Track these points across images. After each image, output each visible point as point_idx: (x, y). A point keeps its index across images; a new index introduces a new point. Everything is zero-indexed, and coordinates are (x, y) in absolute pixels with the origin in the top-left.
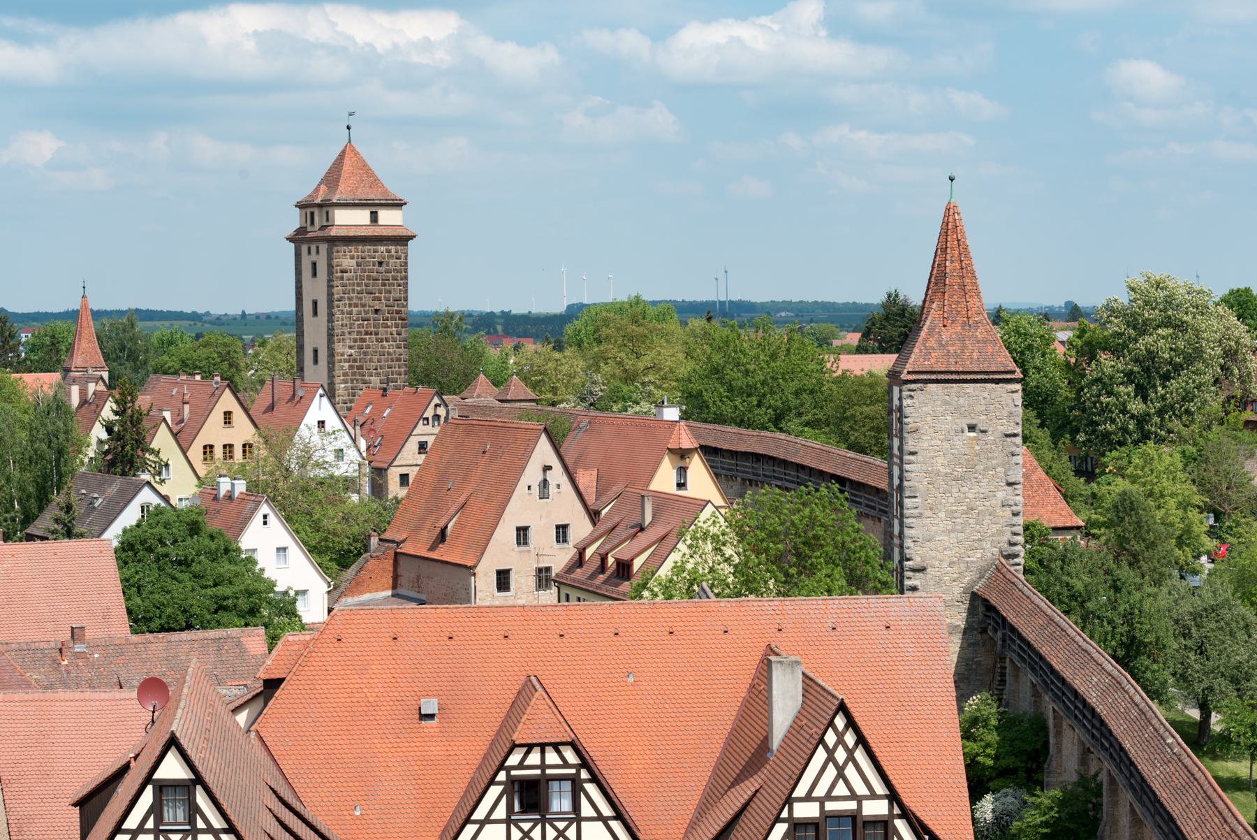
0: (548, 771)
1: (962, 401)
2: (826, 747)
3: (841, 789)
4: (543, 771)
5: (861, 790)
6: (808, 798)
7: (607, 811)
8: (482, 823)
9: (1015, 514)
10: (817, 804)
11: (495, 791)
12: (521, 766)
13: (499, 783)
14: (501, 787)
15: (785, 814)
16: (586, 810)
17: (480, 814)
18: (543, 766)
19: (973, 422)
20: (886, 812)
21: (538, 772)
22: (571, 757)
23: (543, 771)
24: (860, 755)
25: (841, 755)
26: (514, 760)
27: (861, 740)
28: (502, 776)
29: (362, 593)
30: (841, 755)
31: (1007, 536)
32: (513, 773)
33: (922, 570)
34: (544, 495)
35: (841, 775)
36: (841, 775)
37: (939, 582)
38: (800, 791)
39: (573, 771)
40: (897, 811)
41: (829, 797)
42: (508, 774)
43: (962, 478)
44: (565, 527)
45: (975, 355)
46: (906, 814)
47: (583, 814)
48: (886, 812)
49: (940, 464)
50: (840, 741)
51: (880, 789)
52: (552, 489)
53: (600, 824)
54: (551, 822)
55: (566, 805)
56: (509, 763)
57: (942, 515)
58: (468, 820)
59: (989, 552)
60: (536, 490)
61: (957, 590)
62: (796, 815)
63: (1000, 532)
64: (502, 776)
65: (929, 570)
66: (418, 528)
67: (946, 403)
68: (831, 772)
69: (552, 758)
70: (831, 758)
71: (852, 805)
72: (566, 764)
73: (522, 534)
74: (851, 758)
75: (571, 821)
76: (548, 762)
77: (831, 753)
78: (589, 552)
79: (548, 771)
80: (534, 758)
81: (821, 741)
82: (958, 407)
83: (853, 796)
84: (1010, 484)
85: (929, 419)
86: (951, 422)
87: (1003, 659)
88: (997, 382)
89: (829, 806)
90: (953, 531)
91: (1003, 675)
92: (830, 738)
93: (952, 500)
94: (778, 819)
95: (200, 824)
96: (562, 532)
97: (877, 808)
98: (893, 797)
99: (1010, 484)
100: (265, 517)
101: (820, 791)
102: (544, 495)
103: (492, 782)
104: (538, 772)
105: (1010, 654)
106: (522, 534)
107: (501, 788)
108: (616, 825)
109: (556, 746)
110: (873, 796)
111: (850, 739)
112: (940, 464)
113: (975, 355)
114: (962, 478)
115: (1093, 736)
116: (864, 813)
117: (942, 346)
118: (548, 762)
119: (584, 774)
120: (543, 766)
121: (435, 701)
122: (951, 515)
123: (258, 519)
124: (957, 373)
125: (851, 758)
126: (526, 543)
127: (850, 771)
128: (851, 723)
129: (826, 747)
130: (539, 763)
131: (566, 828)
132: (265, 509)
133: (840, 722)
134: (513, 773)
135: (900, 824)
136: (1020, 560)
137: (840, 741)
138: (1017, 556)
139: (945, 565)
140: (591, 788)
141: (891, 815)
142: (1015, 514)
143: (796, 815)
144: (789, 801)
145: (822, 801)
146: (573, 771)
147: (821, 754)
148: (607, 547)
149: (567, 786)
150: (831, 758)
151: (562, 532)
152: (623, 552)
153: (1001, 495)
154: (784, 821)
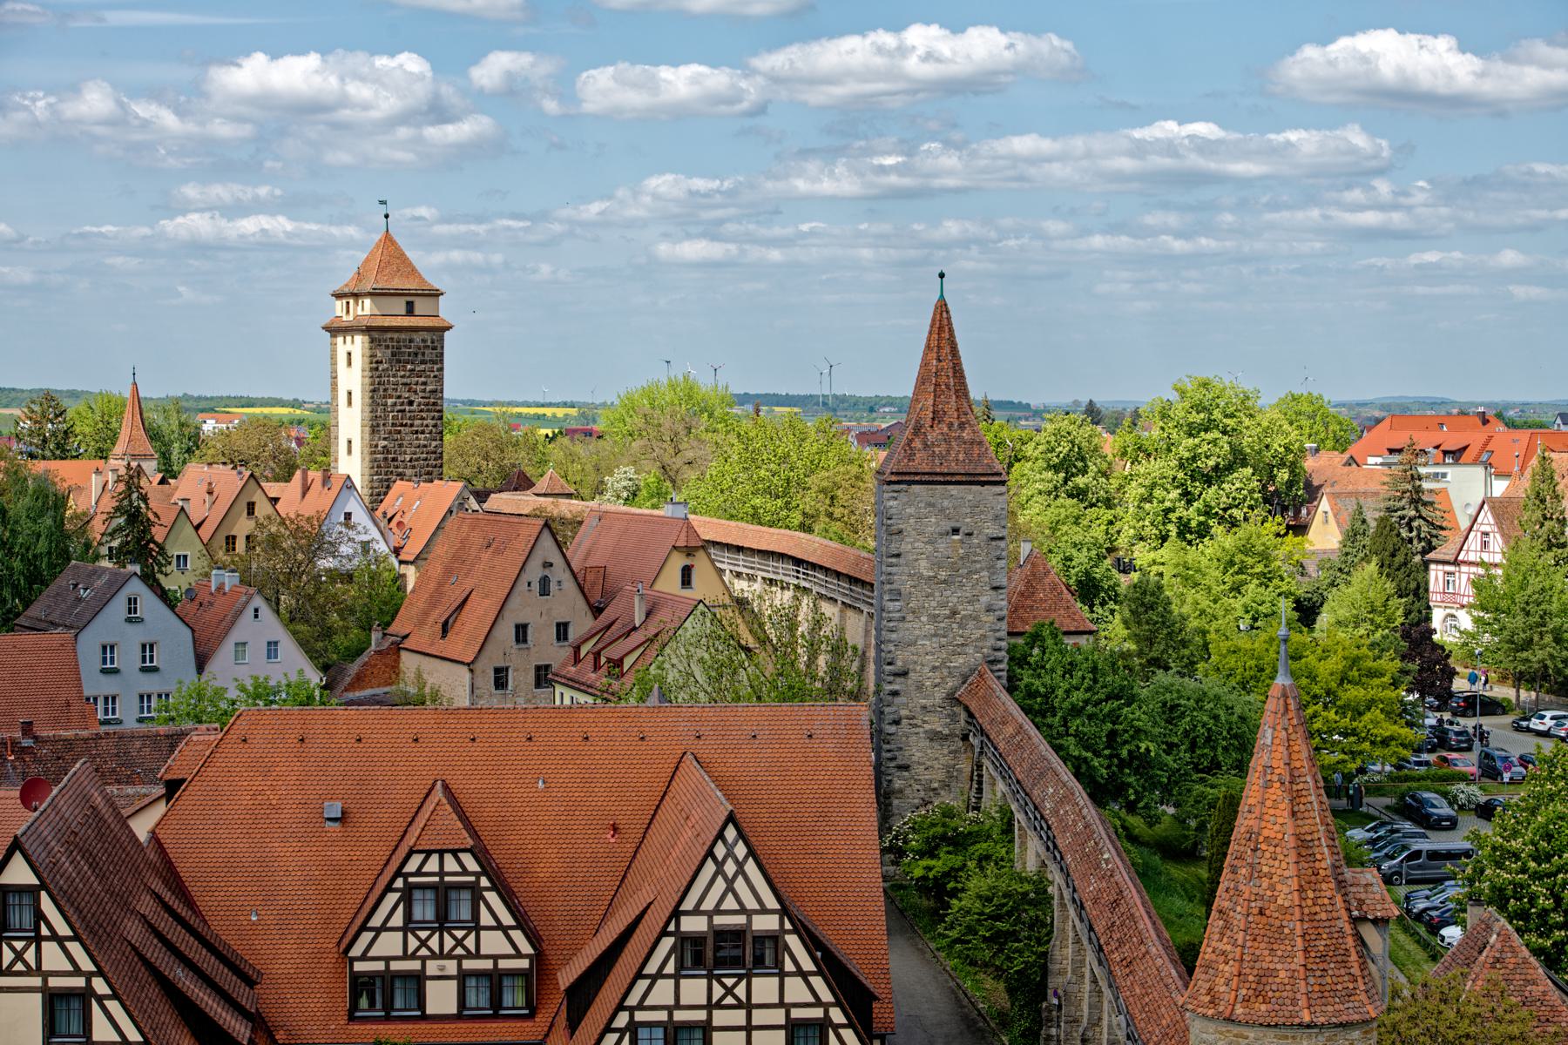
0: (447, 879)
1: (946, 503)
2: (715, 859)
3: (730, 904)
4: (442, 879)
5: (751, 904)
6: (696, 911)
7: (507, 920)
8: (378, 931)
9: (1000, 619)
10: (705, 918)
11: (392, 898)
12: (419, 873)
13: (396, 890)
14: (398, 895)
15: (672, 928)
16: (486, 919)
17: (376, 921)
18: (442, 873)
19: (957, 525)
20: (776, 927)
21: (437, 879)
22: (472, 865)
23: (442, 879)
24: (751, 867)
25: (730, 868)
26: (412, 866)
27: (751, 852)
28: (399, 883)
29: (363, 688)
30: (730, 868)
31: (991, 642)
32: (411, 879)
33: (904, 674)
34: (545, 592)
35: (730, 888)
36: (730, 888)
37: (920, 687)
38: (688, 905)
39: (472, 879)
40: (788, 926)
41: (717, 911)
42: (405, 881)
43: (945, 582)
44: (566, 625)
45: (961, 457)
46: (801, 929)
47: (483, 922)
48: (776, 927)
49: (924, 567)
50: (730, 853)
51: (772, 903)
52: (553, 587)
53: (500, 933)
54: (449, 930)
55: (466, 914)
56: (407, 869)
57: (924, 619)
58: (364, 927)
59: (973, 657)
60: (536, 587)
61: (939, 694)
62: (683, 929)
63: (984, 637)
64: (399, 883)
65: (911, 674)
66: (421, 623)
67: (930, 505)
68: (720, 885)
69: (451, 864)
70: (720, 871)
71: (741, 920)
72: (465, 872)
73: (521, 632)
74: (740, 870)
75: (470, 930)
76: (447, 869)
77: (720, 865)
78: (583, 652)
79: (447, 879)
80: (433, 865)
81: (710, 853)
82: (942, 510)
83: (743, 910)
84: (995, 588)
85: (912, 521)
86: (933, 524)
87: (980, 767)
88: (983, 484)
89: (719, 920)
90: (935, 635)
91: (980, 783)
92: (720, 851)
93: (934, 604)
94: (664, 933)
95: (45, 931)
96: (562, 630)
97: (766, 923)
98: (784, 911)
99: (995, 588)
100: (256, 610)
101: (709, 904)
102: (545, 592)
103: (389, 888)
104: (437, 879)
105: (986, 762)
106: (521, 632)
107: (398, 895)
108: (517, 936)
109: (455, 853)
110: (764, 911)
111: (741, 850)
112: (924, 567)
113: (961, 457)
114: (945, 582)
115: (1048, 849)
116: (755, 927)
117: (926, 446)
118: (447, 869)
119: (484, 882)
120: (442, 873)
121: (339, 805)
122: (934, 618)
123: (250, 612)
124: (917, 474)
125: (740, 870)
126: (525, 641)
127: (740, 884)
128: (741, 835)
129: (715, 859)
130: (437, 869)
131: (465, 937)
132: (258, 602)
133: (731, 833)
134: (411, 879)
135: (793, 941)
136: (1004, 666)
137: (730, 853)
138: (1000, 662)
139: (926, 670)
140: (492, 897)
141: (783, 931)
142: (1000, 619)
143: (683, 929)
144: (676, 914)
145: (710, 915)
146: (472, 879)
148: (600, 646)
149: (466, 895)
150: (720, 871)
151: (562, 630)
152: (614, 652)
153: (984, 599)
154: (669, 934)
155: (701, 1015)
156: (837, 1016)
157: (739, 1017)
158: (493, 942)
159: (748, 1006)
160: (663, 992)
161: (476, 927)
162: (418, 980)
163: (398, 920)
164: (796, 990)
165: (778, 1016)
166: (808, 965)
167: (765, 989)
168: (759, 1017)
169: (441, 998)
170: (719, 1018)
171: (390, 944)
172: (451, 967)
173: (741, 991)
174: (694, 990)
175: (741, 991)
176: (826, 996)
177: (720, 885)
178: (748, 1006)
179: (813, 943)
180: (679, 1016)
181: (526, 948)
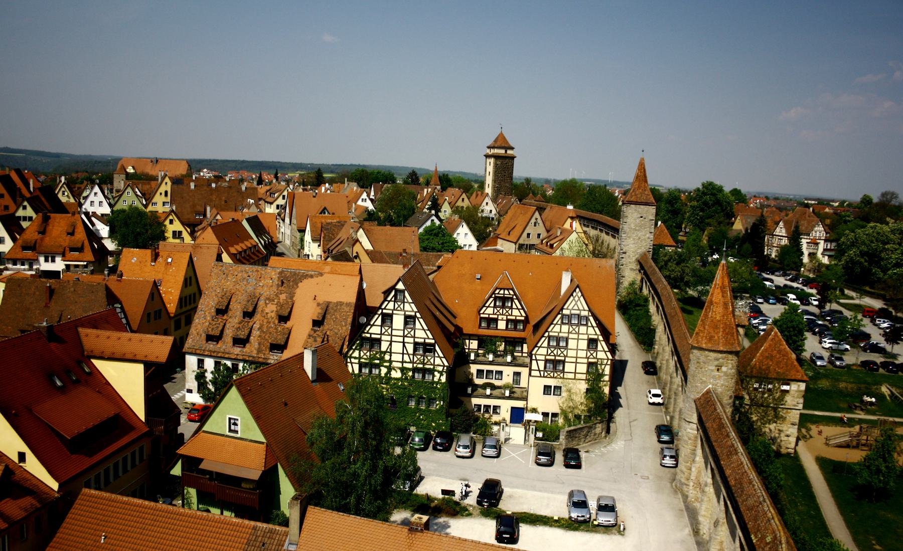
5: (581, 308)
7: (520, 307)
16: (514, 306)
22: (511, 292)
24: (582, 299)
25: (577, 298)
26: (497, 292)
30: (577, 298)
49: (633, 226)
51: (587, 308)
69: (506, 292)
73: (528, 235)
96: (539, 235)
98: (590, 310)
101: (570, 307)
102: (535, 225)
108: (522, 311)
111: (580, 294)
112: (633, 226)
127: (579, 303)
133: (578, 290)
135: (591, 318)
140: (516, 301)
144: (562, 309)
147: (572, 298)
151: (539, 235)
152: (552, 242)
155: (566, 335)
156: (601, 338)
157: (576, 336)
158: (516, 312)
159: (579, 334)
160: (557, 328)
161: (511, 308)
162: (496, 320)
163: (492, 305)
164: (591, 331)
165: (586, 337)
166: (594, 325)
167: (583, 329)
168: (581, 337)
169: (502, 325)
170: (571, 336)
171: (490, 310)
172: (505, 318)
173: (577, 330)
174: (565, 328)
175: (577, 330)
176: (598, 333)
177: (574, 303)
178: (579, 334)
179: (596, 319)
180: (561, 335)
181: (524, 314)
